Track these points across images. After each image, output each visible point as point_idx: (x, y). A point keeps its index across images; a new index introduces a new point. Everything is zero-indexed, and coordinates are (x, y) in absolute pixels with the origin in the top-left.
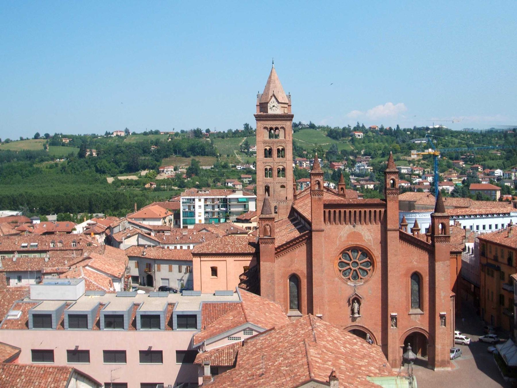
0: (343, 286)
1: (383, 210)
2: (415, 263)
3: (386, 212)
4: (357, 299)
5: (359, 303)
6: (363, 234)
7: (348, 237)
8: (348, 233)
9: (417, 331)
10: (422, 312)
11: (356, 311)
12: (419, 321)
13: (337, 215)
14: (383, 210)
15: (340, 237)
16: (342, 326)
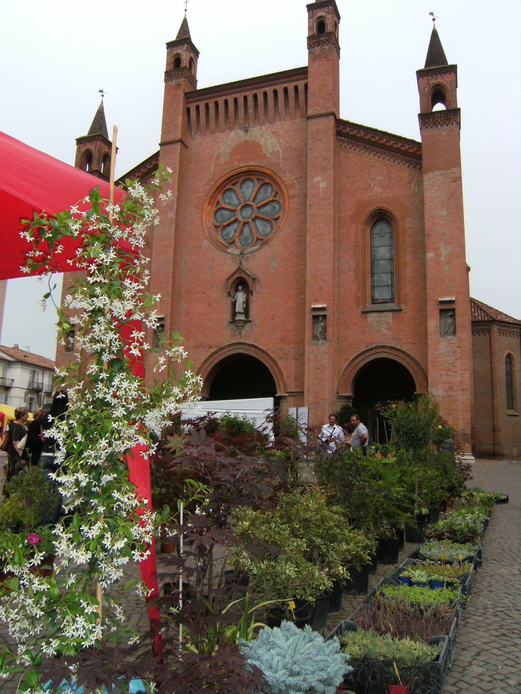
0: (218, 255)
1: (301, 84)
2: (377, 190)
3: (306, 86)
4: (241, 282)
5: (248, 292)
6: (262, 143)
7: (232, 154)
8: (234, 144)
9: (384, 356)
10: (397, 308)
11: (239, 308)
12: (389, 329)
13: (212, 111)
14: (301, 84)
15: (218, 156)
16: (210, 347)
